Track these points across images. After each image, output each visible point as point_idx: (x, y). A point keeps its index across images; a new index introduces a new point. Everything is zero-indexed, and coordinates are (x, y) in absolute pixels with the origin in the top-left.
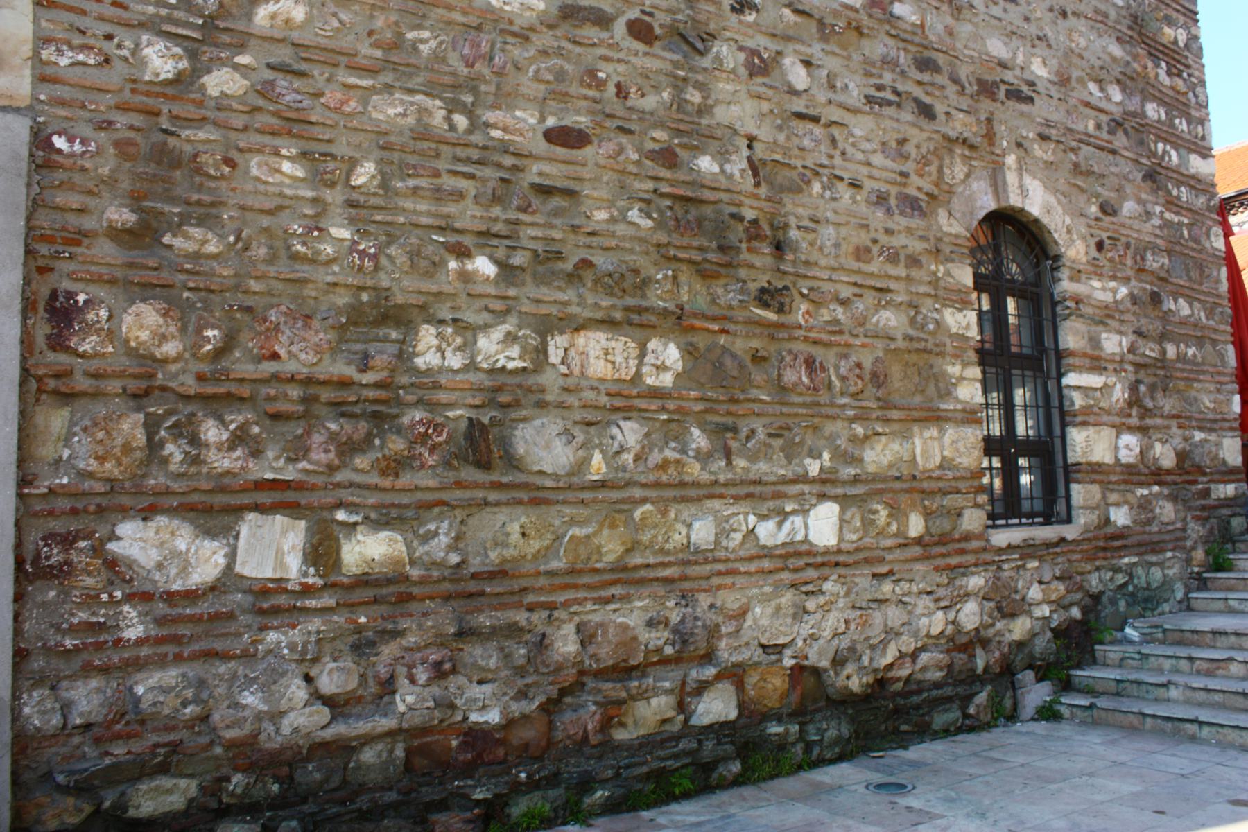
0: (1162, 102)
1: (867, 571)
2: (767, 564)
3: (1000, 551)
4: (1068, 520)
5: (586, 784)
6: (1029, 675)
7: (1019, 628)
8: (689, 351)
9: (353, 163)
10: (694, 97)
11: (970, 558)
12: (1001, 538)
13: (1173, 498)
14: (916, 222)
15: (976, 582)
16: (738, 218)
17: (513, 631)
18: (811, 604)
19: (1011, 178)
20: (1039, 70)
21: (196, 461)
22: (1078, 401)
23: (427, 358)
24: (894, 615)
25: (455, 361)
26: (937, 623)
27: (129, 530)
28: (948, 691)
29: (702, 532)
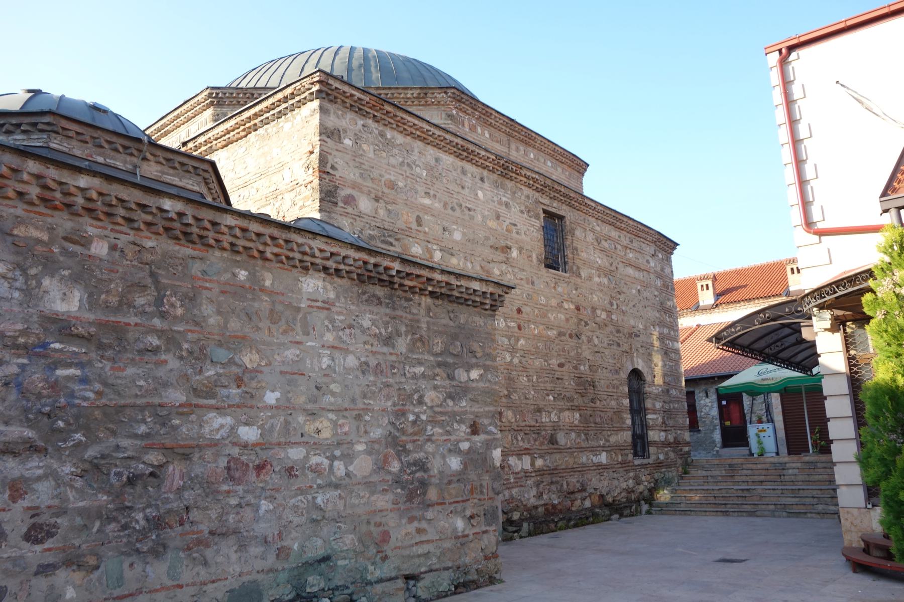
0: (668, 328)
1: (611, 470)
2: (595, 468)
3: (636, 466)
4: (649, 458)
5: (570, 520)
6: (643, 502)
7: (641, 488)
8: (580, 415)
9: (533, 376)
10: (579, 351)
11: (630, 468)
12: (638, 462)
13: (674, 452)
14: (617, 376)
15: (632, 474)
16: (587, 381)
17: (557, 482)
18: (602, 478)
19: (635, 359)
20: (641, 326)
21: (517, 444)
22: (651, 423)
23: (544, 420)
24: (616, 482)
25: (548, 420)
26: (624, 485)
27: (510, 458)
28: (627, 504)
29: (584, 459)
